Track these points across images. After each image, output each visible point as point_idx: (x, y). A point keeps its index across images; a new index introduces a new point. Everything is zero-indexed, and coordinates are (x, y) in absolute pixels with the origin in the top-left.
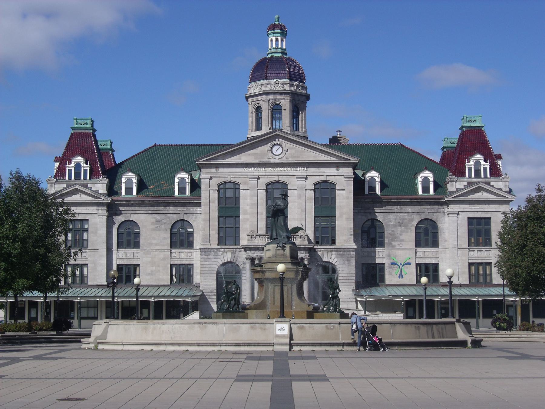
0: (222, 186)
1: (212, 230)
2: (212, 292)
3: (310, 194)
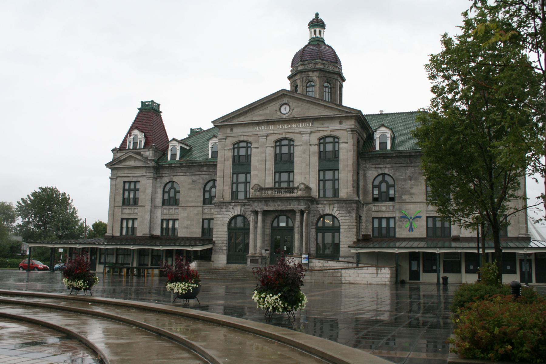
0: (236, 146)
1: (226, 186)
2: (223, 243)
3: (315, 148)
